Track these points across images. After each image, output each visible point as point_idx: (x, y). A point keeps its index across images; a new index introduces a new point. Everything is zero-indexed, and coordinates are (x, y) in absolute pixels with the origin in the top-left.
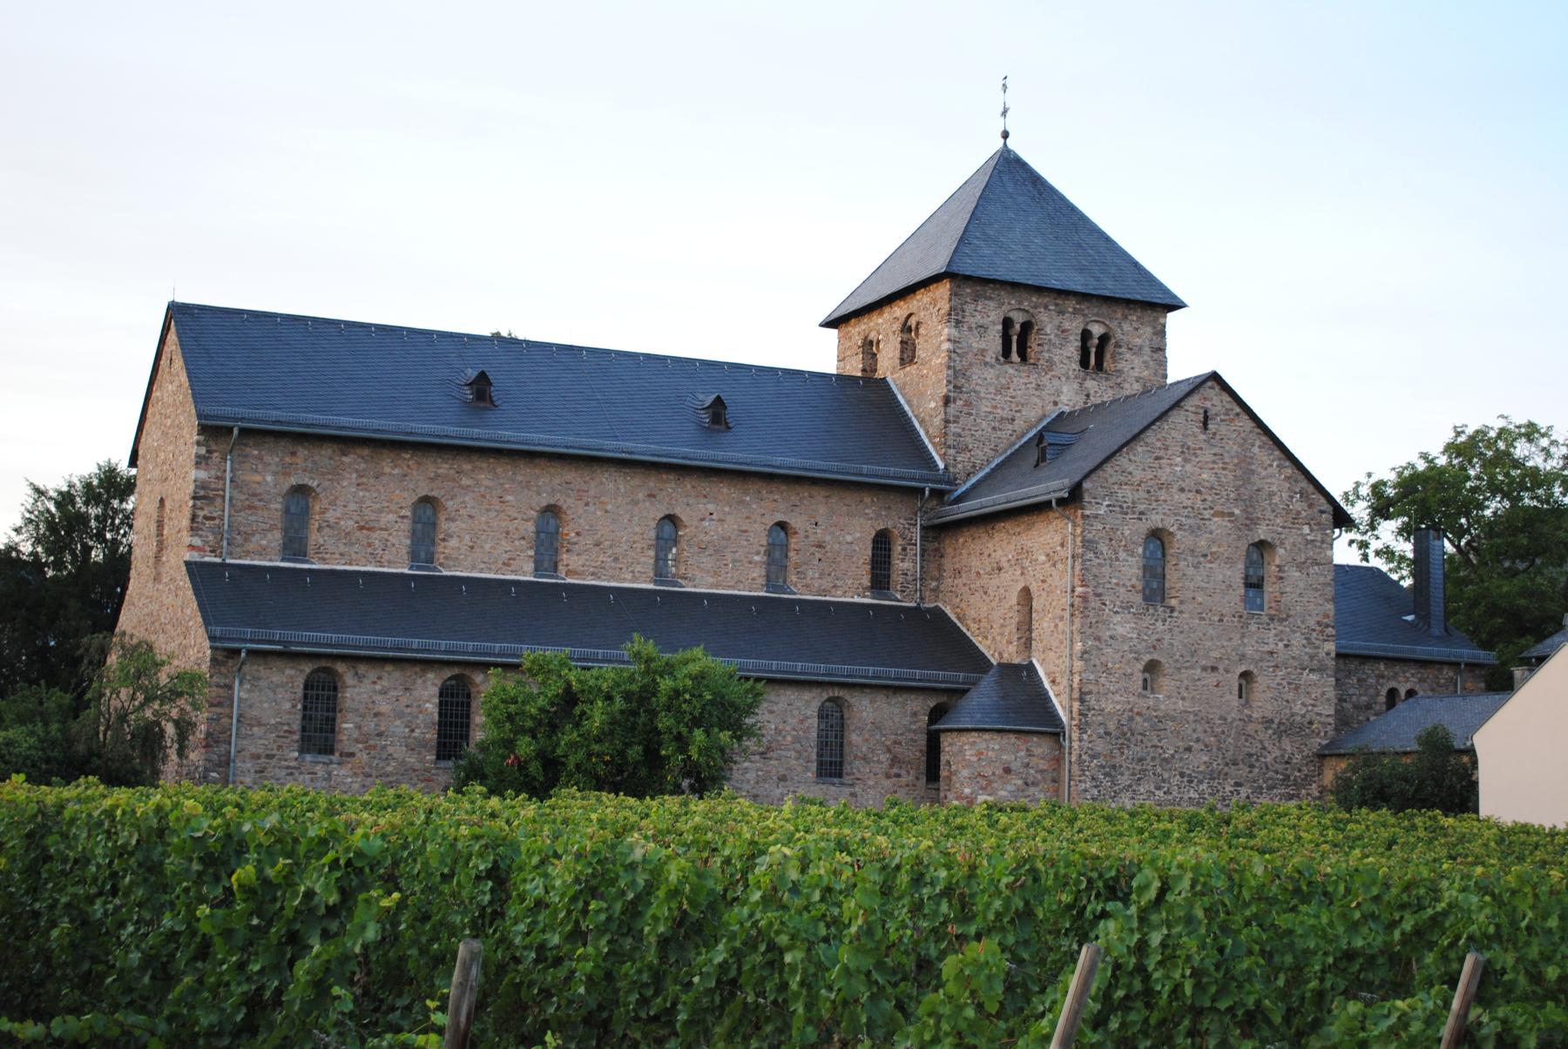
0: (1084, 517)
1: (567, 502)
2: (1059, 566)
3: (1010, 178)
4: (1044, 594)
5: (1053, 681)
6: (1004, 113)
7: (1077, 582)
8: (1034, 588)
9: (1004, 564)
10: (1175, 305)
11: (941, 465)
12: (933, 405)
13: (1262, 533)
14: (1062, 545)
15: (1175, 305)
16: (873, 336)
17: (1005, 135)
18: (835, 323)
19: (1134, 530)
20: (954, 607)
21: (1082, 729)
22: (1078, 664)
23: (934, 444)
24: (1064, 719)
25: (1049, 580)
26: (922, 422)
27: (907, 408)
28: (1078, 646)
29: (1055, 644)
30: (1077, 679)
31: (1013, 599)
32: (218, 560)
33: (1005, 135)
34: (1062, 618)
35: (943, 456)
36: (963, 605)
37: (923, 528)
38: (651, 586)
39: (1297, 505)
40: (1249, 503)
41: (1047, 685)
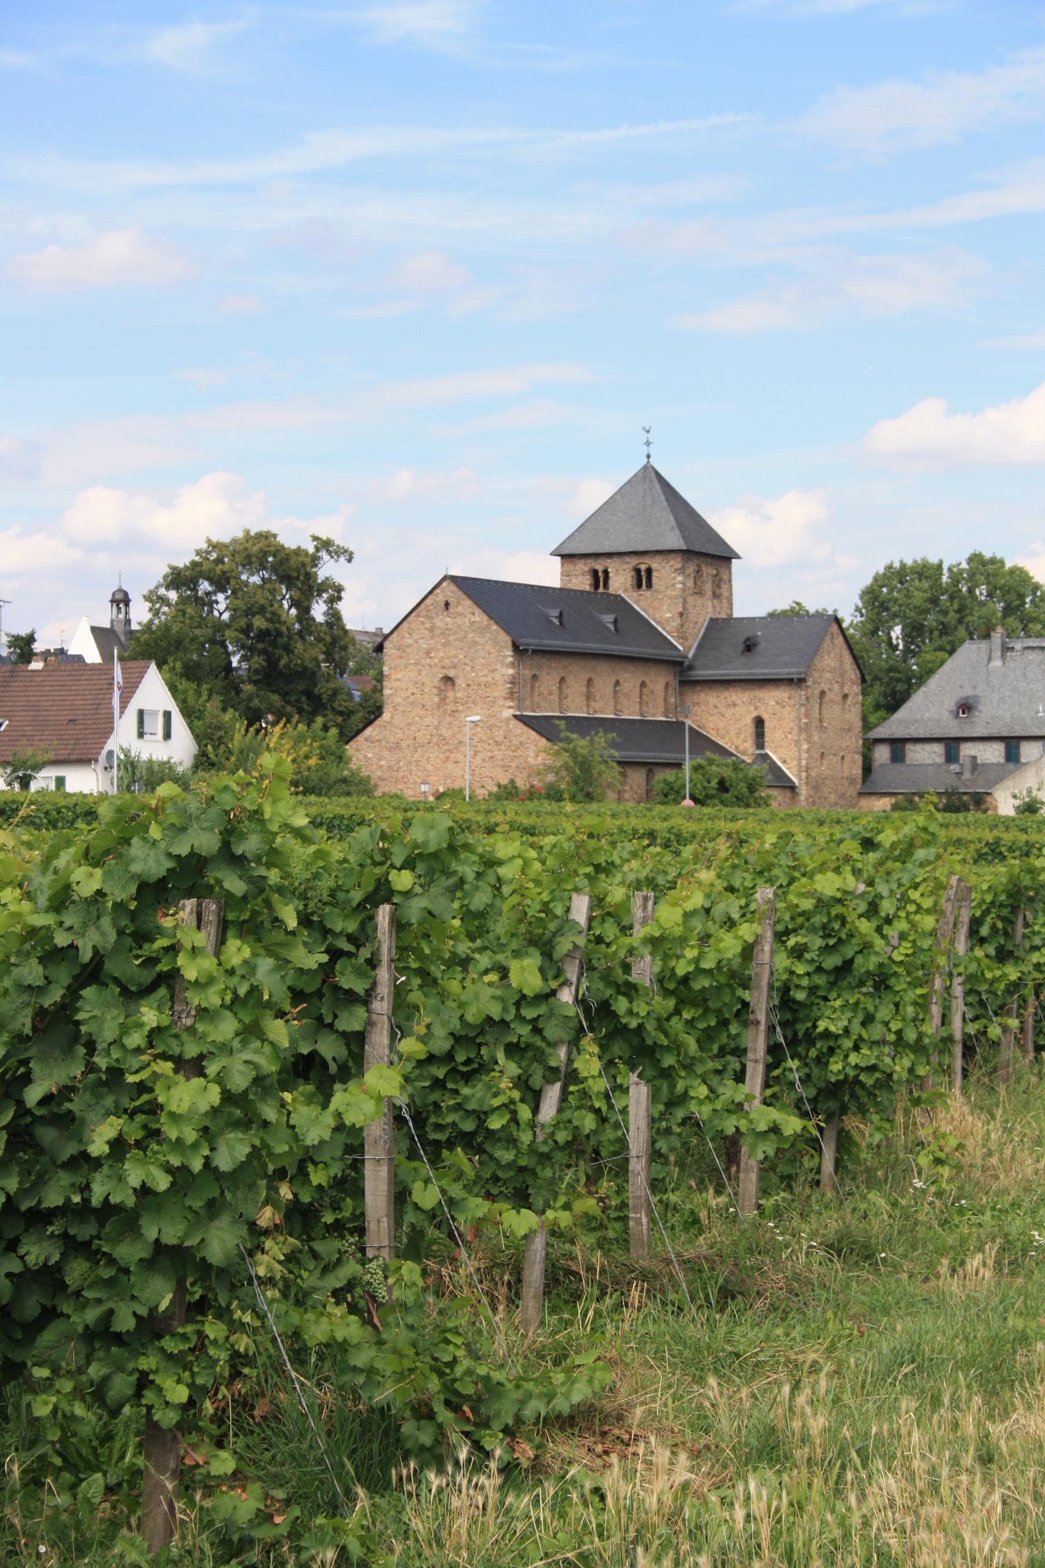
1: (594, 677)
3: (652, 482)
5: (784, 762)
6: (648, 444)
8: (765, 716)
9: (738, 702)
10: (738, 557)
11: (681, 648)
13: (846, 691)
15: (738, 557)
16: (600, 568)
17: (648, 456)
18: (567, 557)
19: (817, 692)
20: (694, 722)
24: (795, 780)
26: (658, 623)
28: (805, 747)
30: (804, 763)
31: (748, 721)
33: (648, 456)
40: (842, 675)
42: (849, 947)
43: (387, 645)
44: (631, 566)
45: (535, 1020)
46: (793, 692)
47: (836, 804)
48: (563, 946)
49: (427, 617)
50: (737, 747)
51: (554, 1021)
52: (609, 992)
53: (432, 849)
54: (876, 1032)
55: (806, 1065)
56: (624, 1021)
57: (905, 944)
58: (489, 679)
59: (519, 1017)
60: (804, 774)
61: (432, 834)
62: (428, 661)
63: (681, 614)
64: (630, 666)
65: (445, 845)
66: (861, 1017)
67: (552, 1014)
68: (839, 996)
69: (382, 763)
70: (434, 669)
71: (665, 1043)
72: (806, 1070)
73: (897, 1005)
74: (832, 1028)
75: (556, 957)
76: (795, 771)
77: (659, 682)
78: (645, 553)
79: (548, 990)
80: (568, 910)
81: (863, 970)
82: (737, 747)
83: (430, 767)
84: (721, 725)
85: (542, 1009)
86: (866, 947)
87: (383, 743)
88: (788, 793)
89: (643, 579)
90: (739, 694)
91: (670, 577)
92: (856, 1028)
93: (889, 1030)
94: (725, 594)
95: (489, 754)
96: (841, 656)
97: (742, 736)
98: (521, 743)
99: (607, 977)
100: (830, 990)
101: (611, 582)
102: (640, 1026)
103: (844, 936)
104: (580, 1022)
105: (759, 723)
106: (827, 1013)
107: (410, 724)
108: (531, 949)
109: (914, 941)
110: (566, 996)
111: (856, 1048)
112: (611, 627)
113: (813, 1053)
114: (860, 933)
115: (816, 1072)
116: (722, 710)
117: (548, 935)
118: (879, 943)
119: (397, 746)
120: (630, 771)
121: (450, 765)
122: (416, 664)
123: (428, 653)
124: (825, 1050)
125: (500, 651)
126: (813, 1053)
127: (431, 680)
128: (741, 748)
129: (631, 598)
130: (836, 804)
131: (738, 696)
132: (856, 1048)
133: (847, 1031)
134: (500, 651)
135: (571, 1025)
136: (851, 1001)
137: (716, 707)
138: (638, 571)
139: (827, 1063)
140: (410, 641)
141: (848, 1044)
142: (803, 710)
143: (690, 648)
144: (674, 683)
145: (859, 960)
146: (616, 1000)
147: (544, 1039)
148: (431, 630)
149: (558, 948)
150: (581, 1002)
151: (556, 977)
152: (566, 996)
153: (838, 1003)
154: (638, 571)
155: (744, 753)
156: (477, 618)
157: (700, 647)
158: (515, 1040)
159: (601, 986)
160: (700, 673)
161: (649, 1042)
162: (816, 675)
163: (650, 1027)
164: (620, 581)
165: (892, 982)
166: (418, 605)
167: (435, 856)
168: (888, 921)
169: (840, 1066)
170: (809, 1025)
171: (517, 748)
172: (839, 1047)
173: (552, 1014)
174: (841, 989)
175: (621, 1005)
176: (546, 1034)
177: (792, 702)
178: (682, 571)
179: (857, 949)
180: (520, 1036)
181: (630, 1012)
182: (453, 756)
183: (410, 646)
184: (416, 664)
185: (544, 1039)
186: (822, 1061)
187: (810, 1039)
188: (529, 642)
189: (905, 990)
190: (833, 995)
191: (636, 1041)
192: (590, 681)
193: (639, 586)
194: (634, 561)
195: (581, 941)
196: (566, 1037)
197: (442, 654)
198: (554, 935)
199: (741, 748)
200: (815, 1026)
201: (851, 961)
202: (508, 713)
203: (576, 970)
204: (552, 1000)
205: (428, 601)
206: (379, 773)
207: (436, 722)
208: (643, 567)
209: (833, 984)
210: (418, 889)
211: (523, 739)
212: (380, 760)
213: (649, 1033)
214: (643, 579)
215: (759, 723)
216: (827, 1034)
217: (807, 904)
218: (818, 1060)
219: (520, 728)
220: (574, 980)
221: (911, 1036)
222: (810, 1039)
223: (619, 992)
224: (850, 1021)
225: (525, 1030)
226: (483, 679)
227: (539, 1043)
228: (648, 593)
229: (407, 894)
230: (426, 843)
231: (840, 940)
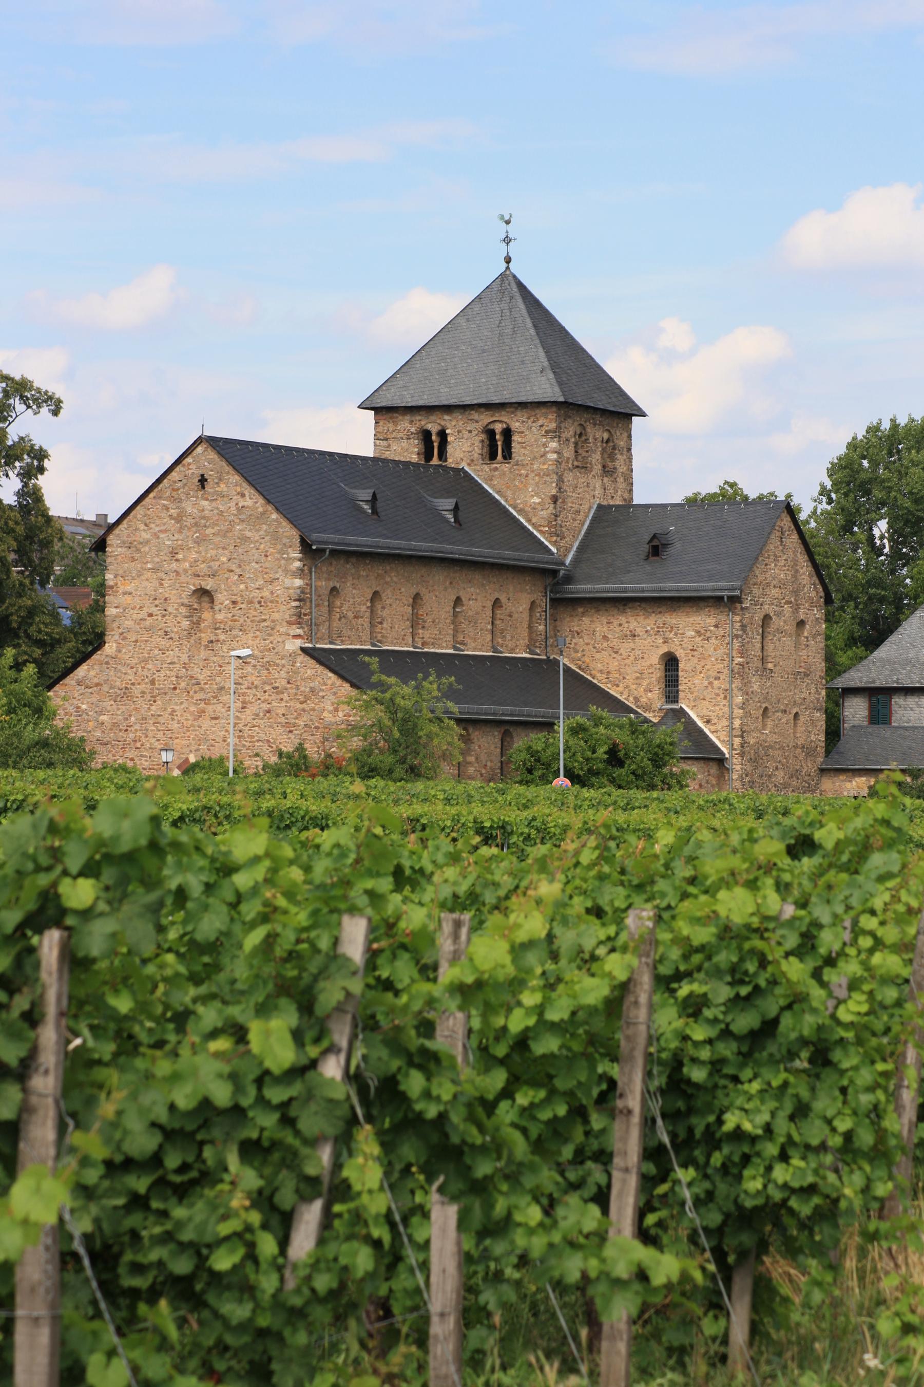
0: (742, 609)
1: (423, 591)
2: (713, 641)
4: (695, 660)
5: (708, 722)
6: (507, 240)
7: (735, 653)
8: (680, 653)
9: (639, 631)
10: (643, 414)
11: (554, 550)
12: (536, 500)
14: (716, 626)
15: (643, 414)
16: (434, 428)
17: (508, 260)
18: (383, 411)
19: (758, 618)
20: (573, 661)
21: (742, 755)
22: (738, 712)
23: (541, 532)
25: (701, 650)
26: (520, 511)
27: (497, 497)
28: (739, 699)
29: (708, 697)
30: (737, 723)
31: (655, 658)
32: (310, 645)
33: (508, 260)
34: (717, 678)
35: (554, 543)
36: (586, 659)
37: (551, 599)
38: (451, 651)
39: (813, 594)
40: (796, 592)
41: (700, 724)
42: (770, 999)
43: (112, 540)
44: (479, 426)
45: (285, 1106)
46: (723, 617)
47: (786, 786)
48: (330, 995)
49: (172, 498)
50: (637, 699)
51: (313, 1107)
52: (395, 1064)
53: (125, 846)
54: (814, 1133)
55: (706, 1176)
56: (418, 1107)
57: (857, 996)
58: (266, 594)
59: (261, 1101)
60: (737, 741)
61: (126, 825)
62: (174, 565)
63: (555, 499)
64: (477, 577)
65: (143, 842)
66: (788, 1107)
67: (309, 1096)
68: (756, 1076)
69: (102, 718)
70: (183, 578)
71: (479, 1141)
72: (707, 1185)
73: (844, 1091)
74: (747, 1126)
75: (319, 1011)
76: (723, 735)
77: (521, 600)
78: (501, 406)
79: (304, 1061)
80: (336, 942)
81: (793, 1036)
82: (637, 699)
83: (175, 726)
84: (614, 665)
85: (295, 1089)
86: (796, 1001)
87: (105, 688)
88: (714, 769)
89: (498, 446)
90: (641, 619)
91: (538, 443)
92: (782, 1126)
93: (834, 1130)
94: (622, 469)
95: (265, 706)
96: (795, 562)
97: (645, 683)
98: (312, 690)
99: (394, 1043)
100: (742, 1066)
101: (450, 449)
102: (442, 1117)
103: (763, 983)
104: (352, 1108)
105: (671, 662)
106: (739, 1101)
107: (146, 661)
108: (283, 1002)
109: (871, 993)
110: (332, 1069)
111: (784, 1157)
112: (450, 517)
113: (717, 1159)
114: (788, 980)
115: (722, 1188)
116: (615, 643)
117: (306, 978)
118: (817, 993)
119: (126, 693)
120: (475, 734)
122: (155, 570)
123: (174, 553)
124: (736, 1158)
125: (281, 552)
126: (717, 1159)
127: (178, 595)
128: (644, 700)
129: (480, 473)
130: (786, 786)
131: (638, 621)
132: (784, 1157)
133: (768, 1129)
134: (281, 552)
135: (339, 1113)
136: (775, 1083)
137: (605, 638)
138: (491, 434)
139: (739, 1178)
140: (146, 536)
141: (771, 1149)
142: (736, 644)
143: (568, 550)
144: (544, 602)
145: (787, 1021)
146: (407, 1075)
147: (297, 1133)
148: (178, 519)
149: (322, 998)
150: (354, 1078)
151: (317, 1040)
152: (332, 1069)
153: (755, 1086)
154: (491, 434)
155: (648, 708)
156: (248, 502)
157: (581, 549)
158: (254, 1135)
159: (384, 1053)
160: (583, 588)
161: (455, 1139)
162: (756, 591)
163: (456, 1118)
164: (464, 448)
165: (837, 1055)
166: (159, 481)
167: (130, 857)
168: (831, 961)
169: (758, 1184)
170: (711, 1118)
172: (758, 1154)
173: (309, 1096)
174: (758, 1064)
175: (414, 1083)
176: (302, 1125)
177: (721, 632)
178: (556, 433)
179: (783, 1002)
180: (262, 1130)
181: (427, 1095)
182: (210, 708)
183: (148, 542)
184: (155, 570)
185: (297, 1133)
186: (732, 1172)
187: (712, 1140)
188: (328, 538)
189: (856, 1068)
190: (747, 1073)
191: (435, 1138)
192: (417, 597)
193: (493, 456)
194: (485, 418)
195: (356, 986)
196: (331, 1131)
198: (316, 978)
199: (644, 700)
200: (720, 1122)
201: (775, 1022)
202: (293, 645)
203: (347, 1030)
204: (310, 1075)
205: (174, 475)
206: (98, 734)
207: (184, 658)
208: (498, 428)
209: (746, 1057)
210: (102, 906)
212: (101, 713)
213: (455, 1128)
214: (498, 446)
215: (671, 662)
216: (738, 1134)
217: (703, 935)
218: (725, 1169)
219: (311, 668)
220: (344, 1044)
221: (866, 1138)
222: (712, 1140)
223: (411, 1064)
224: (773, 1114)
225: (268, 1121)
227: (290, 1139)
228: (506, 467)
229: (87, 914)
230: (116, 839)
231: (757, 988)
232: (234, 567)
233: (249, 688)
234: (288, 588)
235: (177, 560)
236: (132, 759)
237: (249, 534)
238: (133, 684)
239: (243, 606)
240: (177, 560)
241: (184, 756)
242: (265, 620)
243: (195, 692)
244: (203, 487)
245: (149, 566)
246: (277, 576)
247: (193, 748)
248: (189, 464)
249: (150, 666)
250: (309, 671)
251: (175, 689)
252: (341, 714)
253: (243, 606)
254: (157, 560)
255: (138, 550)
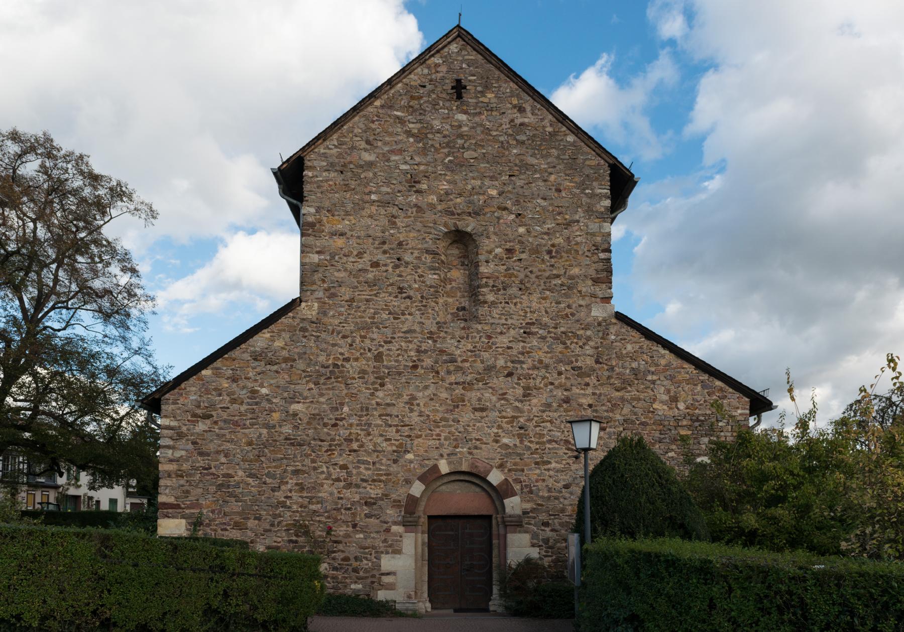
43: (311, 160)
58: (559, 240)
62: (413, 199)
69: (295, 407)
70: (429, 216)
83: (415, 418)
87: (300, 365)
95: (559, 393)
98: (635, 372)
107: (367, 328)
119: (335, 372)
120: (575, 426)
121: (466, 416)
122: (384, 204)
123: (413, 182)
125: (582, 186)
140: (368, 157)
148: (420, 137)
156: (529, 119)
171: (625, 384)
182: (473, 395)
183: (371, 164)
184: (383, 204)
197: (445, 186)
206: (287, 429)
211: (640, 364)
212: (293, 400)
226: (546, 241)
232: (509, 204)
233: (534, 368)
234: (593, 235)
235: (418, 192)
236: (344, 467)
237: (533, 161)
238: (347, 360)
239: (523, 256)
240: (418, 192)
241: (430, 463)
242: (558, 276)
243: (449, 372)
244: (459, 97)
245: (373, 197)
246: (577, 217)
247: (445, 452)
248: (437, 65)
249: (375, 336)
250: (629, 347)
251: (415, 367)
252: (681, 406)
253: (523, 256)
254: (385, 189)
255: (356, 176)
